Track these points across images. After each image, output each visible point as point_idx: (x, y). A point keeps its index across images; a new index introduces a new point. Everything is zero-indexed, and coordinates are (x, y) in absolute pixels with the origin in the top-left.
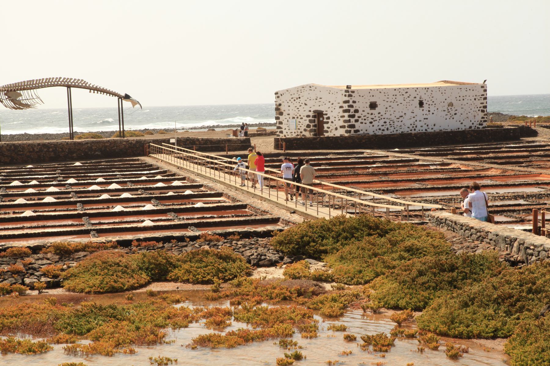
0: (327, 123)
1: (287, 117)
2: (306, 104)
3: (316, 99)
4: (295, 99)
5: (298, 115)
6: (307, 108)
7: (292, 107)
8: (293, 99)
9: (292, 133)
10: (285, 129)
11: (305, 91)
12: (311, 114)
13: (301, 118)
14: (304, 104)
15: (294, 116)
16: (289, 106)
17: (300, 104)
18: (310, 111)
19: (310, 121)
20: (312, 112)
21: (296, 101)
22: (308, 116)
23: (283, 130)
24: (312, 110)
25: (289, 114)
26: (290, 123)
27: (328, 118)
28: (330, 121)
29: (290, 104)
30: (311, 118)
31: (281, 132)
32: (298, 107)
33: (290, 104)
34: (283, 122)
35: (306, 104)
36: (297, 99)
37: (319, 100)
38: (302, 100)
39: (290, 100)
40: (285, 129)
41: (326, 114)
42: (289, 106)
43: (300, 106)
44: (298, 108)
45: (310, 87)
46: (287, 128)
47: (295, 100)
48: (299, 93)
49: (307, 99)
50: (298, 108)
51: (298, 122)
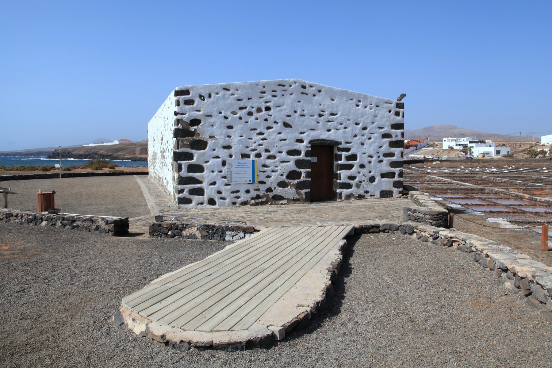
1: (223, 154)
2: (286, 125)
5: (261, 149)
9: (237, 192)
12: (303, 147)
14: (280, 124)
15: (247, 151)
20: (306, 143)
21: (256, 115)
22: (291, 153)
26: (233, 169)
30: (302, 156)
35: (286, 125)
36: (259, 110)
43: (269, 128)
51: (259, 167)
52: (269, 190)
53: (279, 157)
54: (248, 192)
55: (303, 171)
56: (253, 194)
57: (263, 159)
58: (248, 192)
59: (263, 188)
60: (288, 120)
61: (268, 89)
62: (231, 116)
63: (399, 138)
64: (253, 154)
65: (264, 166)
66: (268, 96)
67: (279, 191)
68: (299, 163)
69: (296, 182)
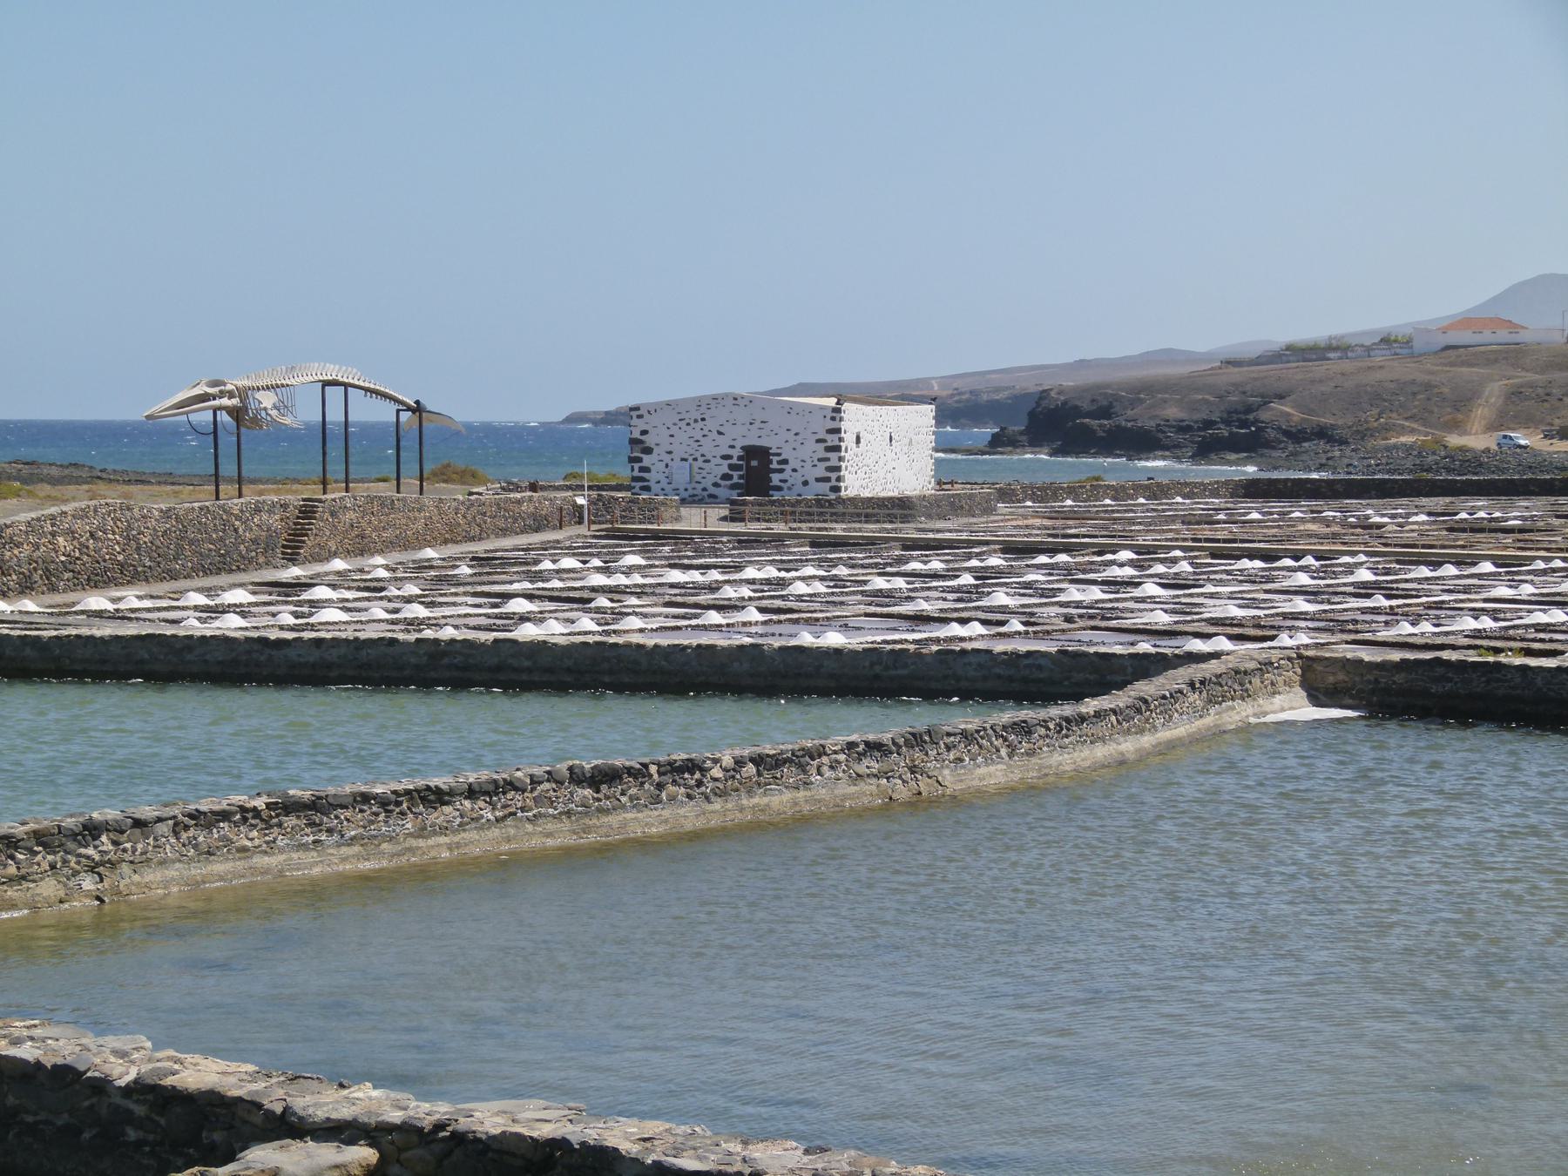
0: (781, 471)
1: (667, 458)
2: (720, 433)
3: (751, 424)
4: (692, 422)
5: (698, 455)
6: (724, 442)
7: (682, 436)
8: (684, 422)
10: (659, 482)
11: (720, 406)
13: (707, 461)
15: (686, 456)
16: (672, 436)
17: (706, 432)
18: (732, 447)
19: (731, 467)
21: (693, 425)
23: (652, 484)
24: (739, 444)
25: (670, 453)
27: (785, 462)
28: (788, 468)
29: (674, 430)
30: (734, 461)
31: (647, 489)
32: (699, 437)
33: (674, 430)
34: (652, 468)
35: (720, 433)
36: (696, 421)
37: (758, 425)
38: (711, 424)
39: (675, 424)
40: (659, 482)
41: (779, 455)
42: (672, 436)
44: (698, 441)
45: (735, 399)
46: (664, 482)
47: (688, 424)
48: (703, 409)
49: (725, 423)
50: (698, 441)
51: (696, 470)
52: (704, 489)
53: (714, 461)
54: (686, 490)
55: (735, 474)
56: (691, 492)
57: (700, 463)
58: (686, 490)
59: (699, 487)
60: (721, 429)
61: (703, 403)
62: (673, 427)
63: (836, 443)
64: (690, 459)
65: (700, 468)
66: (703, 409)
67: (712, 490)
68: (731, 467)
69: (729, 483)
